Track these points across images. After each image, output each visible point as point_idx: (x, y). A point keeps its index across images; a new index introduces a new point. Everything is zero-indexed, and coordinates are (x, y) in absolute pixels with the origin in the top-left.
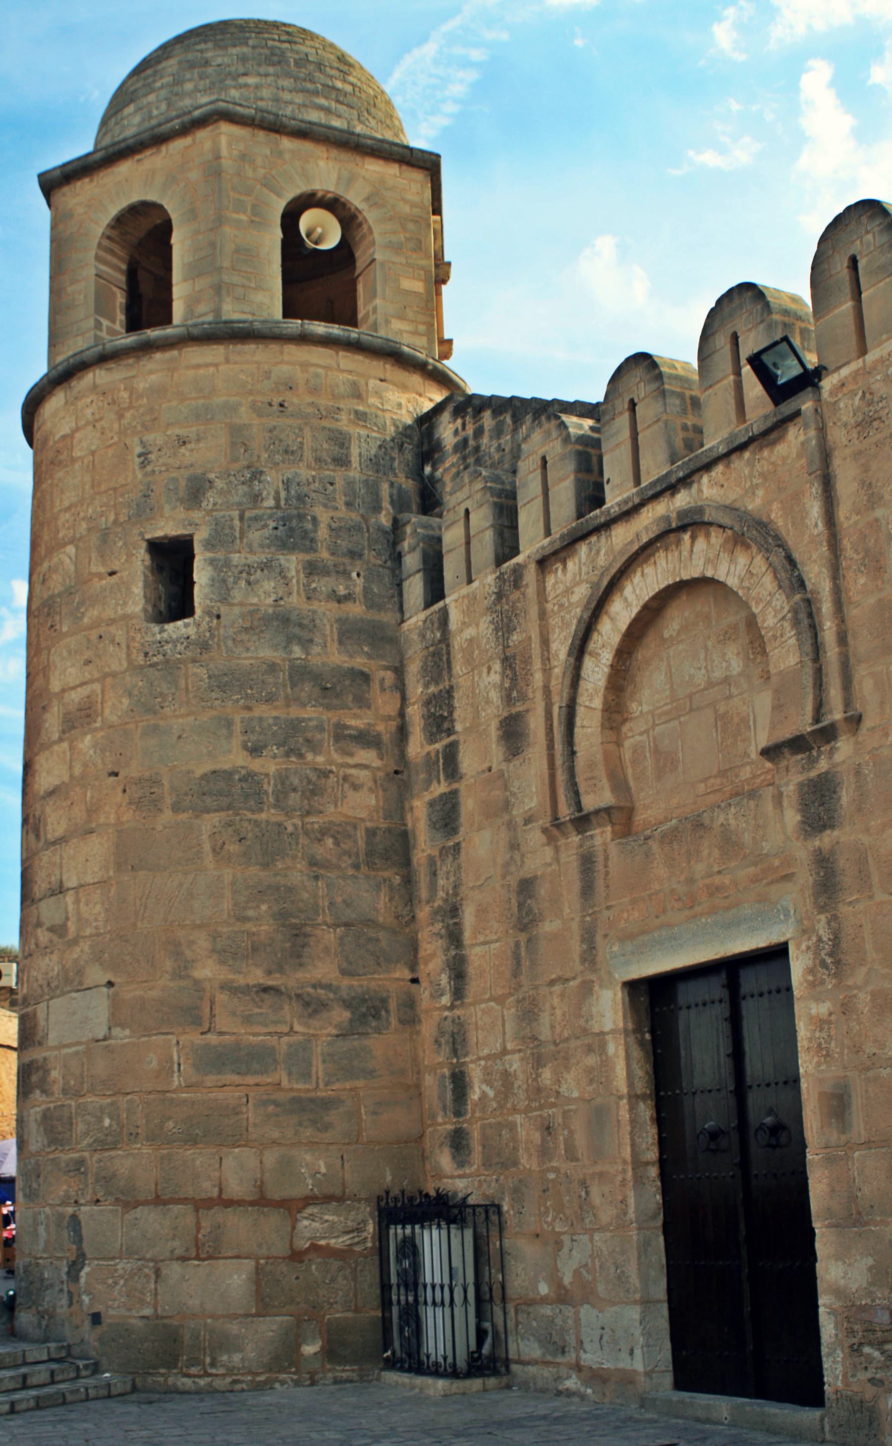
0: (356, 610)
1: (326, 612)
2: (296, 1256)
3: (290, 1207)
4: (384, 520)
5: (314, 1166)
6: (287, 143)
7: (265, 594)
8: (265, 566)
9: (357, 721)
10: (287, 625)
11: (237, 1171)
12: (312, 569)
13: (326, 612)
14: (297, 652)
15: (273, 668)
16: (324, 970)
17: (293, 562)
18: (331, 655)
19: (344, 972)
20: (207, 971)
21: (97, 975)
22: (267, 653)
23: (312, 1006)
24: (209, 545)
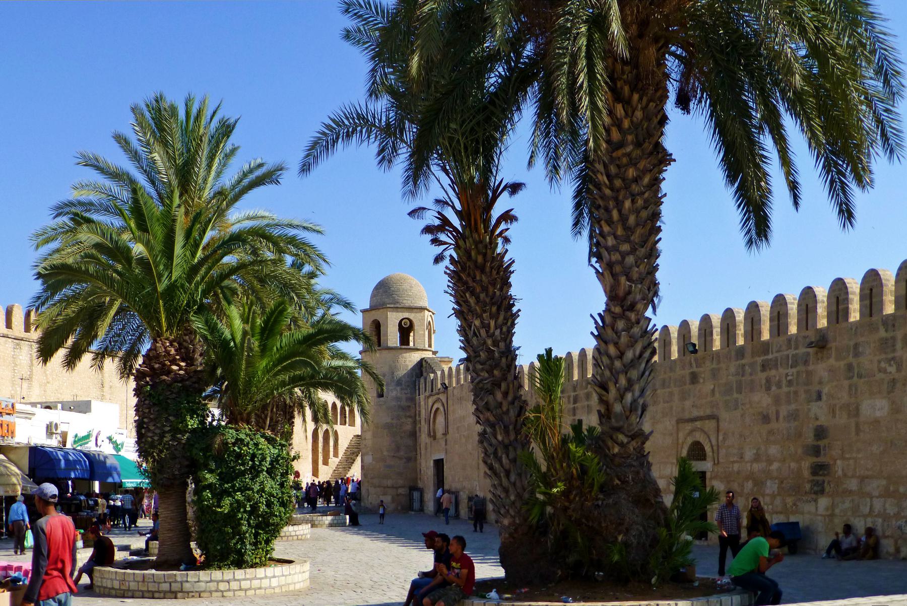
1: (404, 396)
2: (398, 495)
3: (397, 488)
5: (401, 482)
7: (394, 394)
10: (398, 399)
11: (389, 483)
12: (402, 389)
16: (402, 453)
17: (398, 388)
18: (404, 403)
20: (385, 453)
23: (400, 459)
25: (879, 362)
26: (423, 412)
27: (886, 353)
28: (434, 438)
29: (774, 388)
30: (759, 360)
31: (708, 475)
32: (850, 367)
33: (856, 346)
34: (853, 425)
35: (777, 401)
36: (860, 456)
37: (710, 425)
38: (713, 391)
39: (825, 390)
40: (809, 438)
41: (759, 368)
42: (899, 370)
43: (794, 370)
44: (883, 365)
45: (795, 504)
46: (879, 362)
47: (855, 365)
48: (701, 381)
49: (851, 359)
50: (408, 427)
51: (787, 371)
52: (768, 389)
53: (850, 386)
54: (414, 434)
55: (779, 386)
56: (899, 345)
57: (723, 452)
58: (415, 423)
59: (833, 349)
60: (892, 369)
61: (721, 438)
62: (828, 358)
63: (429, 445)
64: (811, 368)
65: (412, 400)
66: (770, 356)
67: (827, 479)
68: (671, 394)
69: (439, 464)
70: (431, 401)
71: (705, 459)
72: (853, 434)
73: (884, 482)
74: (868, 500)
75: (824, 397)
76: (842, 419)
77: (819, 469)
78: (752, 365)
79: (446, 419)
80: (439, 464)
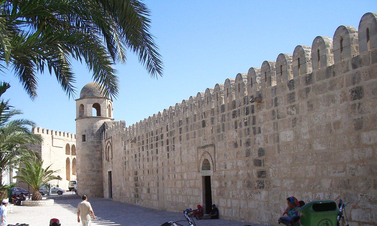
0: (98, 140)
1: (95, 141)
4: (101, 132)
6: (93, 99)
7: (91, 140)
8: (90, 137)
9: (98, 149)
10: (92, 142)
12: (94, 137)
13: (95, 141)
14: (93, 144)
15: (91, 145)
17: (93, 137)
19: (97, 169)
21: (80, 169)
22: (91, 144)
23: (94, 171)
24: (87, 135)
25: (287, 108)
26: (104, 148)
27: (291, 103)
28: (108, 161)
29: (238, 127)
30: (231, 111)
31: (211, 178)
32: (273, 112)
33: (276, 99)
34: (276, 146)
35: (240, 135)
36: (281, 165)
37: (210, 150)
38: (212, 130)
39: (262, 127)
40: (255, 155)
41: (231, 116)
42: (297, 113)
43: (247, 116)
44: (289, 110)
45: (250, 195)
46: (287, 108)
47: (276, 111)
48: (207, 125)
49: (273, 108)
50: (98, 156)
51: (244, 117)
52: (236, 128)
53: (274, 123)
54: (101, 159)
55: (241, 126)
56: (297, 97)
57: (217, 164)
58: (101, 153)
59: (265, 102)
60: (294, 112)
61: (216, 156)
62: (263, 108)
63: (106, 164)
64: (255, 114)
65: (100, 142)
66: (236, 109)
67: (265, 179)
68: (195, 134)
69: (110, 173)
70: (106, 142)
71: (210, 169)
72: (277, 152)
73: (293, 181)
74: (285, 192)
75: (262, 131)
76: (271, 144)
77: (261, 174)
78: (228, 114)
79: (112, 151)
80: (110, 173)
